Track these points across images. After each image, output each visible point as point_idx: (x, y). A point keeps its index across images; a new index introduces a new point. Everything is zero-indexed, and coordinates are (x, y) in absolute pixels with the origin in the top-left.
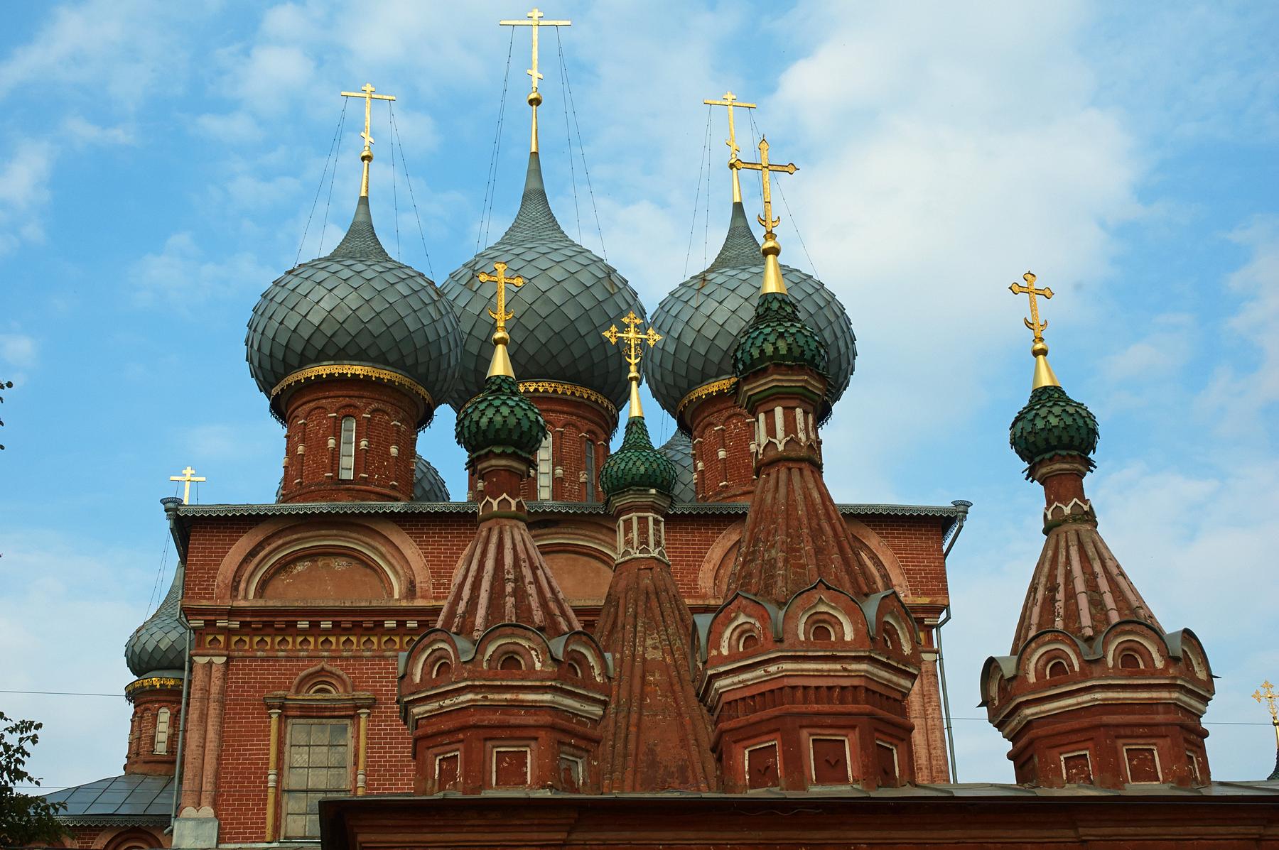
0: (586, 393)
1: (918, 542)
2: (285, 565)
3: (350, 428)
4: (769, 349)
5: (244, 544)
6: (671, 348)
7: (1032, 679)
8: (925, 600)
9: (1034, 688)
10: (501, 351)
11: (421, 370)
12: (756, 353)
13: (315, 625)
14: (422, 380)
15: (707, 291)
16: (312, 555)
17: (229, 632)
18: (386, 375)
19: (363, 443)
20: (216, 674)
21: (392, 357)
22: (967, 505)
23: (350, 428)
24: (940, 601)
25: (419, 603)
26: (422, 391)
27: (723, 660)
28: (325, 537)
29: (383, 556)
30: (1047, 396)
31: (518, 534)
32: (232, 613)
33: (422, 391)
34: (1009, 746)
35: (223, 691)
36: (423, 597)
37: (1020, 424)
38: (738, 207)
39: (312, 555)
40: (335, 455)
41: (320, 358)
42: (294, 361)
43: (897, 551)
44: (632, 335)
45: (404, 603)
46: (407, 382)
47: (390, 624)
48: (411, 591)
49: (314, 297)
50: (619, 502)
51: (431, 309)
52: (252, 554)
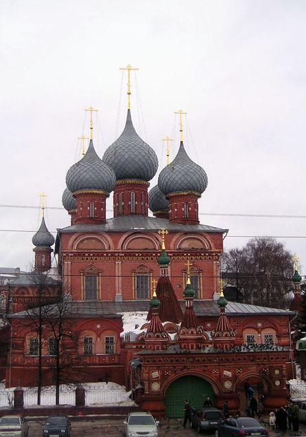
1: (217, 236)
5: (74, 237)
8: (218, 250)
17: (71, 256)
18: (101, 192)
20: (69, 266)
25: (111, 251)
32: (72, 253)
35: (71, 269)
39: (87, 239)
44: (163, 232)
45: (108, 251)
47: (105, 255)
48: (110, 248)
49: (84, 174)
52: (76, 239)
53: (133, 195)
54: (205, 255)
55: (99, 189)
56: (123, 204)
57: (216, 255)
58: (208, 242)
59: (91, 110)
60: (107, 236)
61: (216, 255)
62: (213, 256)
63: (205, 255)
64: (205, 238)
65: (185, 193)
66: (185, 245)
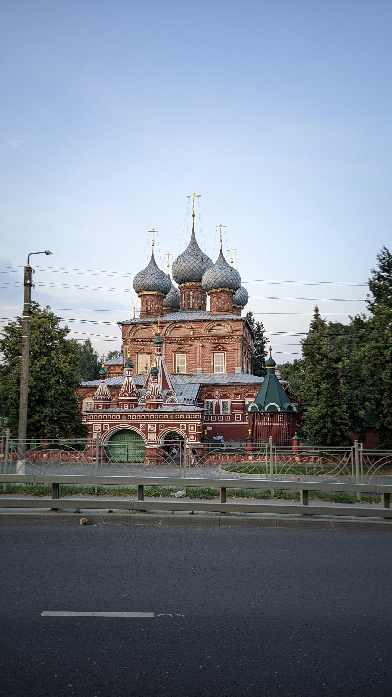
2: (137, 331)
5: (130, 328)
14: (162, 292)
41: (143, 291)
54: (229, 338)
59: (153, 230)
63: (229, 338)
65: (218, 290)
66: (214, 331)
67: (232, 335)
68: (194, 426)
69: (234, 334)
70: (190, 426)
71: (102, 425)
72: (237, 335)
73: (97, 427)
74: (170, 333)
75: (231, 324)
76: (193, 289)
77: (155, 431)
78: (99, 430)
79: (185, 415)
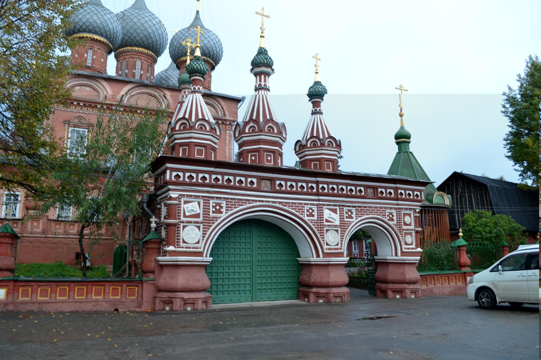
0: (151, 53)
1: (233, 104)
3: (90, 52)
4: (262, 61)
6: (178, 46)
7: (309, 146)
8: (232, 119)
9: (309, 148)
10: (198, 49)
11: (111, 39)
12: (259, 62)
13: (79, 104)
15: (189, 32)
16: (80, 85)
19: (94, 57)
21: (104, 35)
22: (245, 98)
23: (90, 52)
24: (409, 140)
25: (108, 102)
26: (111, 45)
27: (247, 133)
28: (84, 81)
29: (100, 88)
30: (317, 83)
31: (199, 96)
33: (111, 45)
34: (298, 159)
36: (109, 100)
37: (312, 89)
38: (198, 12)
40: (86, 59)
42: (76, 31)
43: (228, 106)
46: (107, 42)
50: (183, 86)
51: (116, 23)
53: (138, 64)
55: (101, 35)
56: (127, 71)
57: (230, 124)
58: (223, 108)
60: (104, 83)
61: (230, 124)
62: (226, 124)
64: (220, 104)
67: (223, 118)
68: (409, 215)
69: (227, 118)
70: (405, 215)
71: (206, 200)
72: (229, 120)
73: (192, 207)
74: (127, 100)
75: (222, 102)
76: (142, 58)
77: (337, 223)
78: (198, 216)
79: (396, 189)
